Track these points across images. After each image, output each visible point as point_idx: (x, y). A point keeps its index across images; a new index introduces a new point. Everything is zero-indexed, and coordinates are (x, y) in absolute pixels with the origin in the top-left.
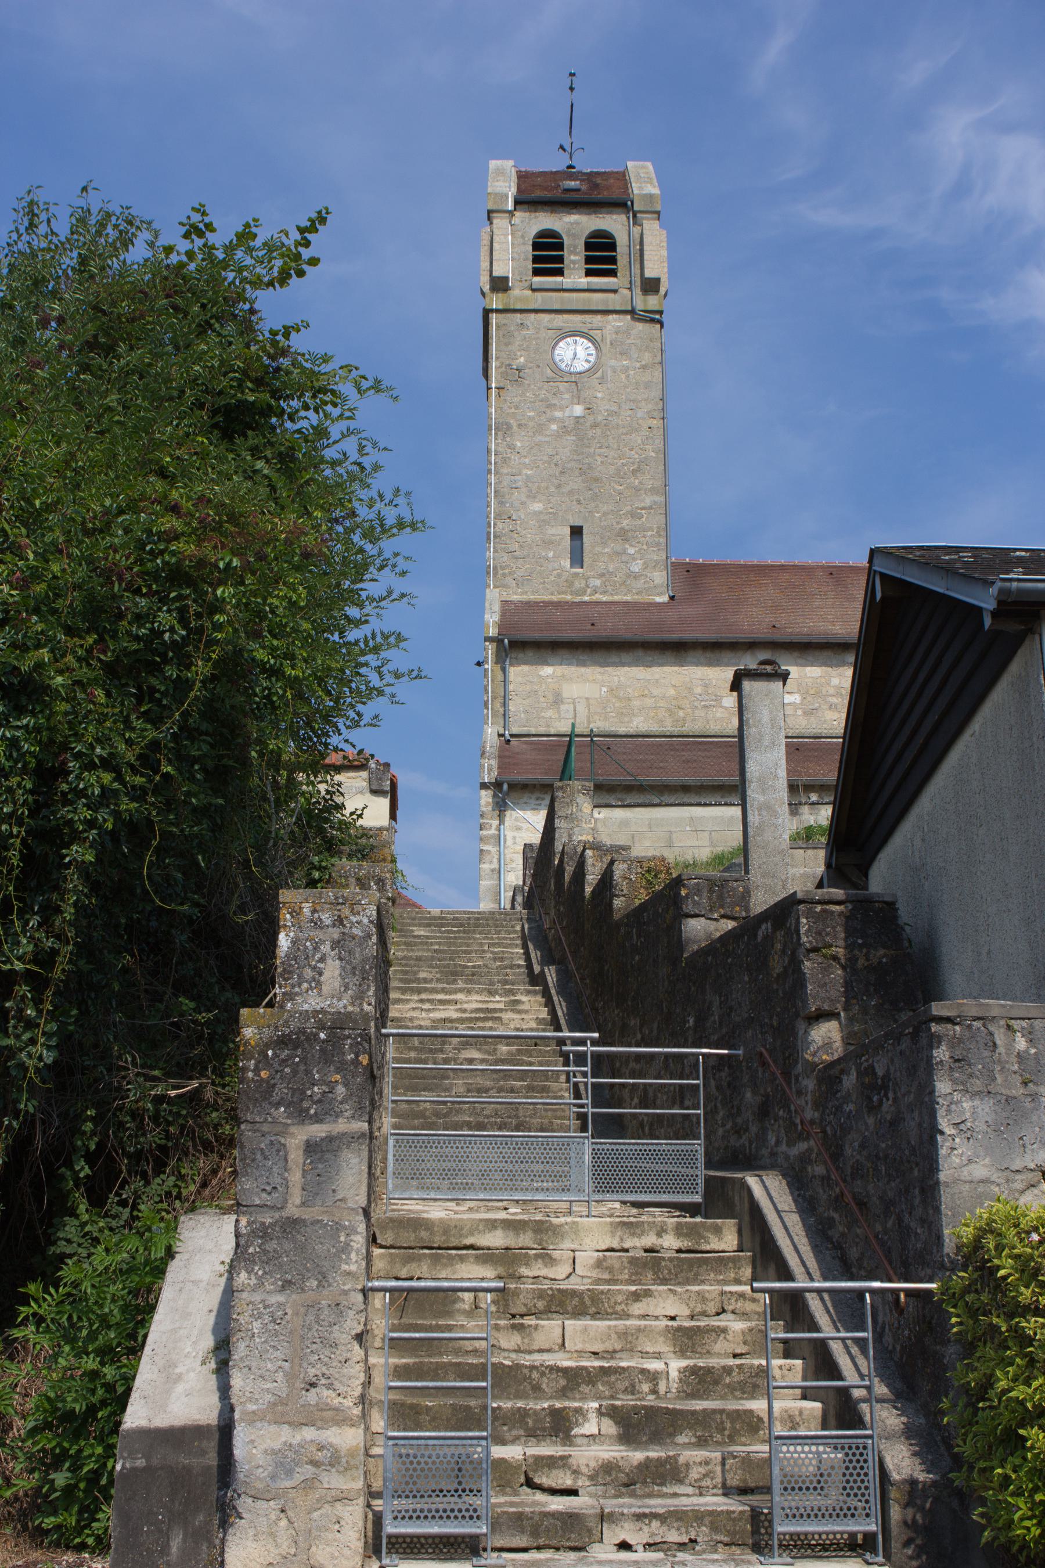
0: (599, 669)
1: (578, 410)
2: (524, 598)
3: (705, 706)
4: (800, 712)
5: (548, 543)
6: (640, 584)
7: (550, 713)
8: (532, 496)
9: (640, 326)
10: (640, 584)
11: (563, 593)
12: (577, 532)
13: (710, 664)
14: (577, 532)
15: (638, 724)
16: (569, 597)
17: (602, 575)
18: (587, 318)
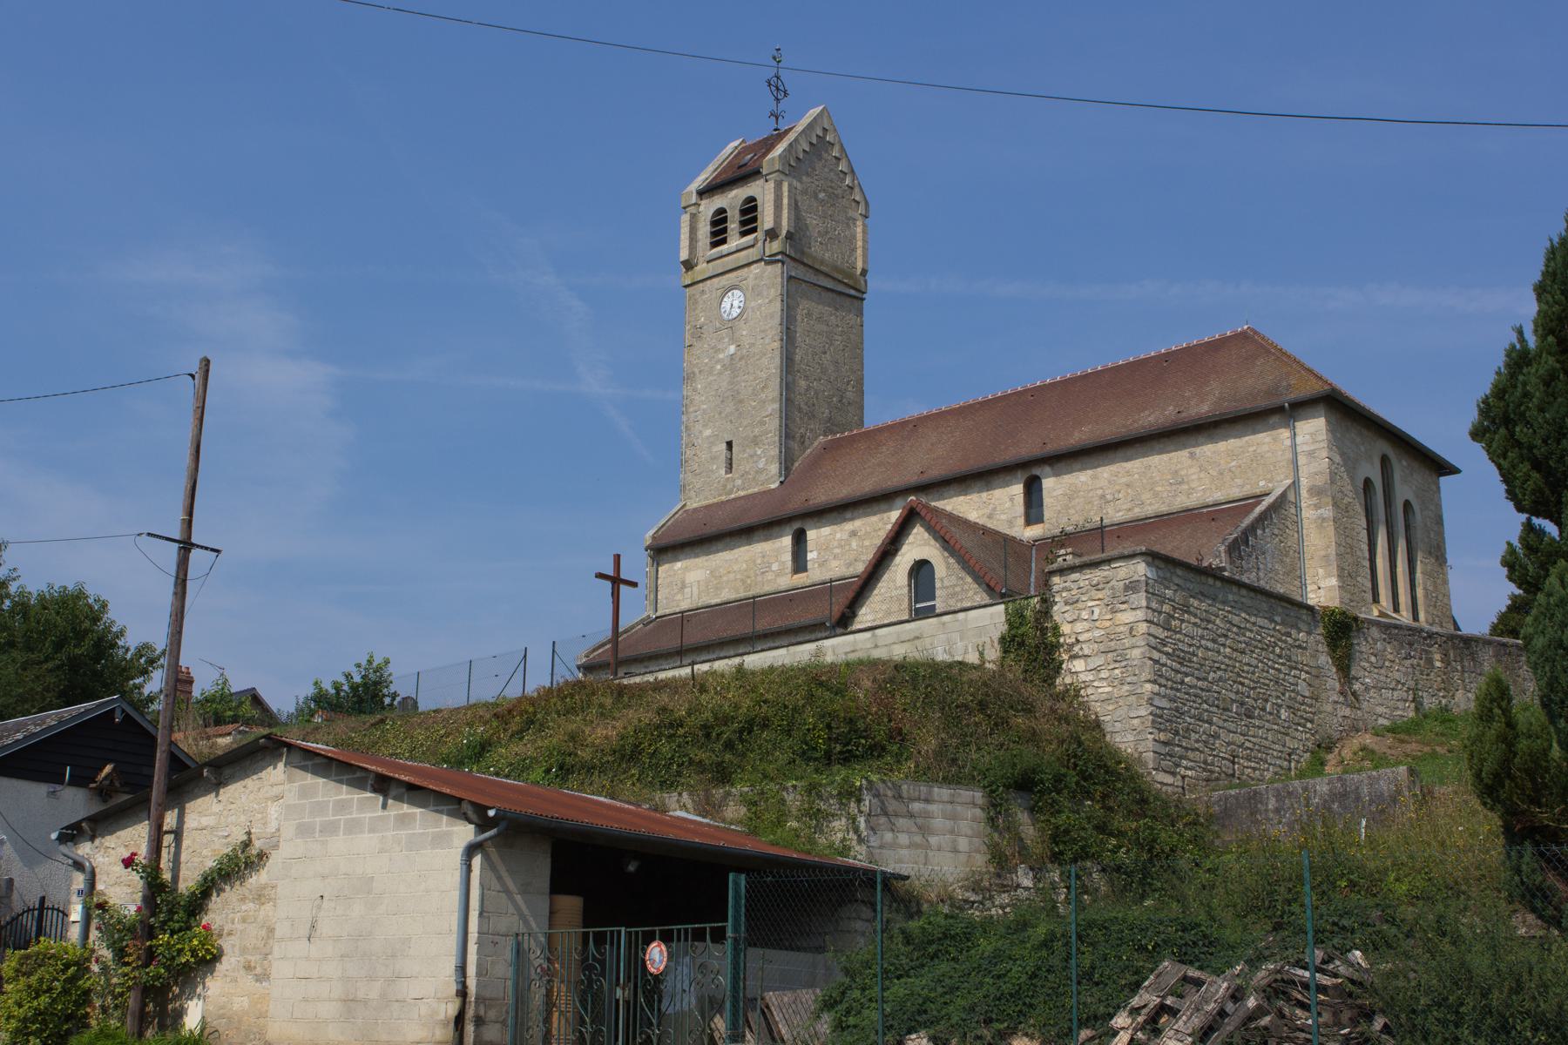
1: (732, 349)
2: (704, 503)
5: (714, 458)
6: (763, 477)
7: (679, 597)
8: (705, 426)
9: (769, 268)
10: (763, 477)
12: (729, 445)
13: (766, 540)
14: (729, 445)
15: (726, 595)
16: (723, 498)
18: (739, 272)
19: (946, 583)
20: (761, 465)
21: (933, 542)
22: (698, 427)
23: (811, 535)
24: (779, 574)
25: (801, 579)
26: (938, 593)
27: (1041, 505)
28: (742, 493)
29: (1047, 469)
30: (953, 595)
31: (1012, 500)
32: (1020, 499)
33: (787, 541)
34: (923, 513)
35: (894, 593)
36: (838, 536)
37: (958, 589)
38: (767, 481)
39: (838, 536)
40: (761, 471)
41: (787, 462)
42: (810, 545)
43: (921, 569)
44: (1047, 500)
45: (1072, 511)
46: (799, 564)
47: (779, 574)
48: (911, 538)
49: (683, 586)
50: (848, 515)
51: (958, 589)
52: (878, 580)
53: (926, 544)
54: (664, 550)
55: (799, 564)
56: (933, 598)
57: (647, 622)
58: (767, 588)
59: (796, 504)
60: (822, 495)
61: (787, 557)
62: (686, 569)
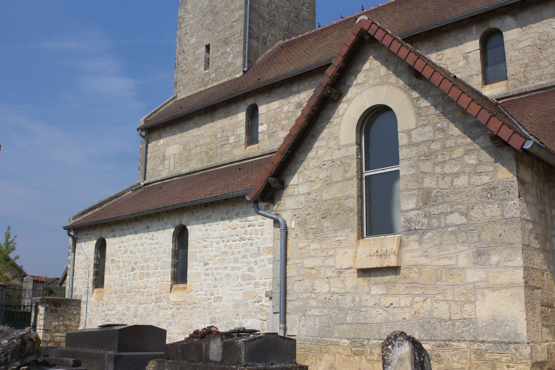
0: (180, 135)
2: (189, 94)
3: (222, 145)
4: (266, 137)
6: (231, 69)
8: (192, 36)
10: (231, 69)
11: (200, 87)
12: (208, 47)
13: (225, 117)
15: (195, 165)
16: (202, 89)
17: (216, 70)
19: (416, 138)
20: (230, 60)
21: (393, 78)
22: (187, 37)
23: (262, 109)
24: (235, 145)
25: (253, 150)
26: (403, 153)
27: (505, 60)
28: (215, 84)
29: (509, 20)
30: (428, 156)
31: (466, 57)
32: (476, 56)
33: (242, 116)
34: (378, 36)
35: (337, 154)
36: (286, 108)
37: (436, 146)
38: (234, 72)
39: (286, 108)
40: (231, 65)
41: (250, 57)
42: (261, 118)
43: (376, 119)
44: (510, 54)
45: (544, 63)
46: (252, 136)
47: (235, 145)
48: (361, 77)
49: (164, 159)
50: (295, 89)
51: (436, 146)
52: (315, 138)
53: (384, 82)
54: (153, 129)
55: (252, 136)
56: (396, 161)
57: (136, 188)
58: (226, 159)
59: (252, 83)
60: (272, 74)
61: (242, 131)
62: (167, 145)
